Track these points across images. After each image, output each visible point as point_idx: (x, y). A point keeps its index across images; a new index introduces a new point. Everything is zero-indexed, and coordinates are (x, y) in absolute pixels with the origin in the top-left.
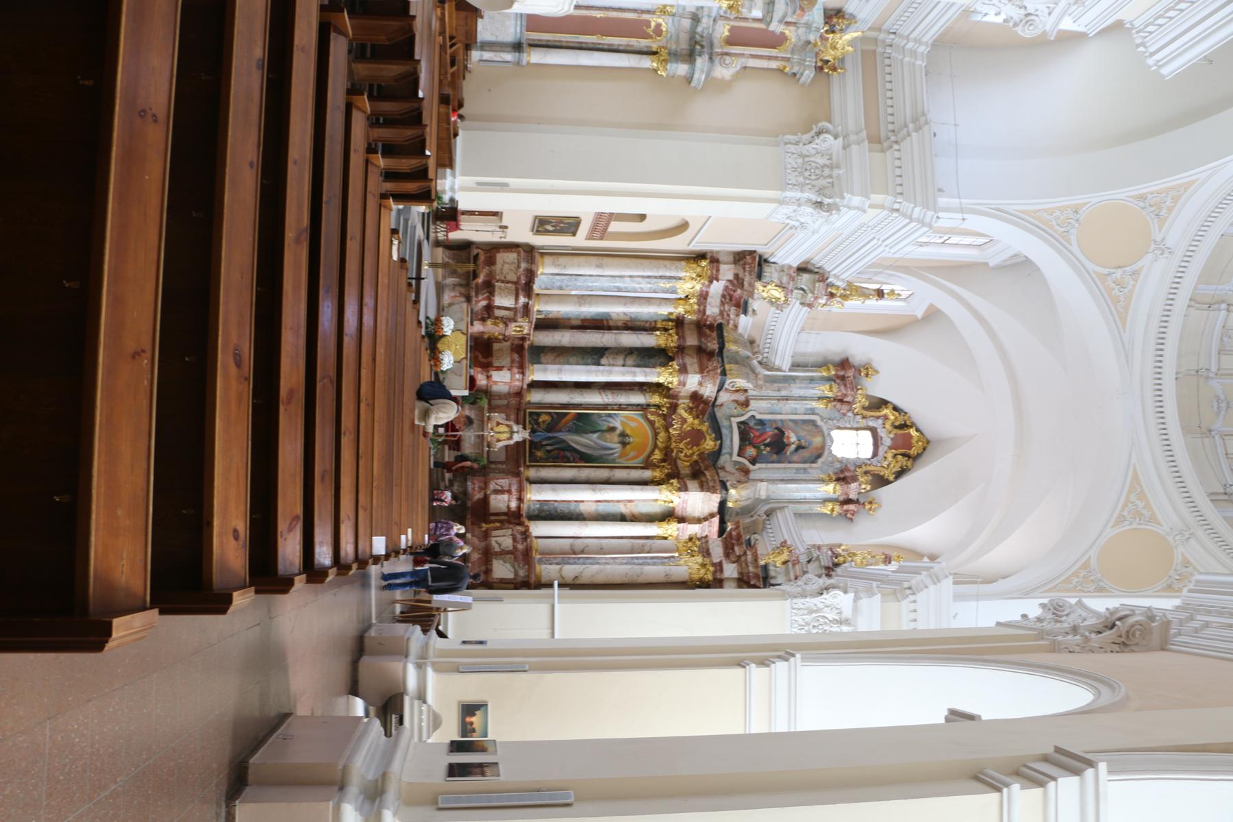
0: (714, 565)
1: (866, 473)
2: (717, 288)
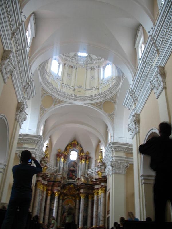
0: (101, 187)
1: (80, 154)
2: (43, 182)
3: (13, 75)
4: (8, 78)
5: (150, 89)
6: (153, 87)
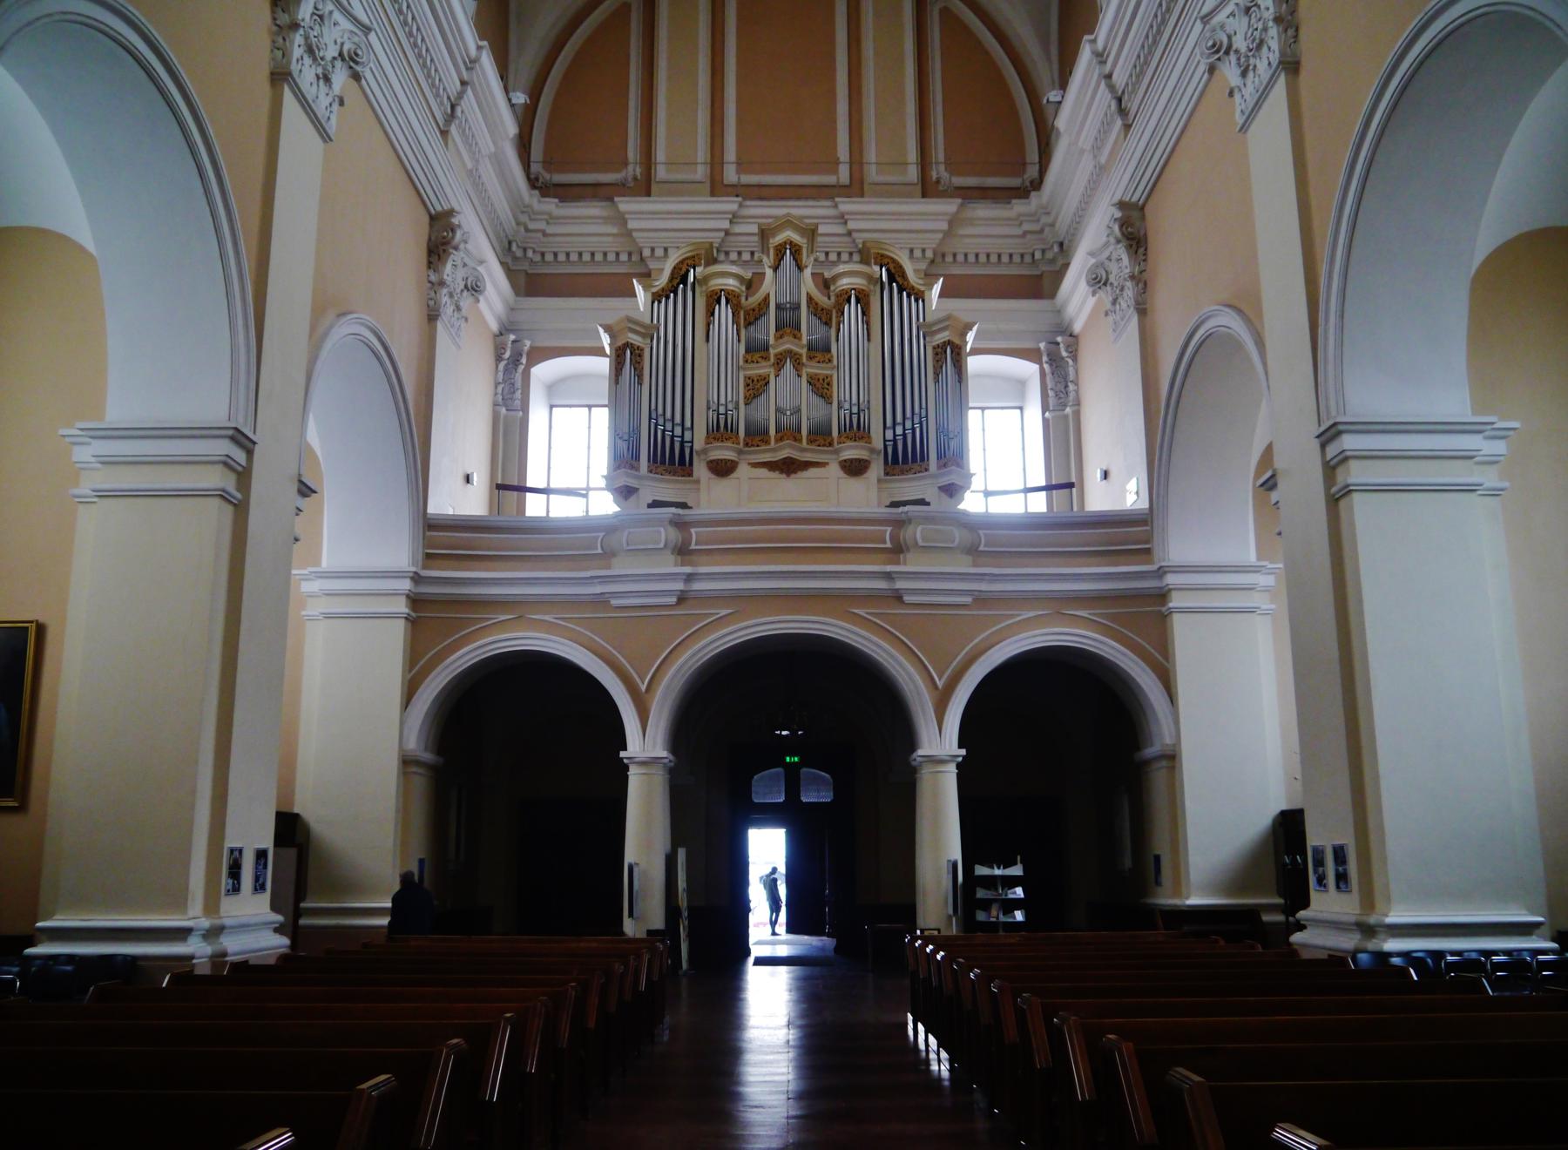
3: (368, 75)
4: (342, 103)
5: (1202, 67)
6: (1221, 50)
